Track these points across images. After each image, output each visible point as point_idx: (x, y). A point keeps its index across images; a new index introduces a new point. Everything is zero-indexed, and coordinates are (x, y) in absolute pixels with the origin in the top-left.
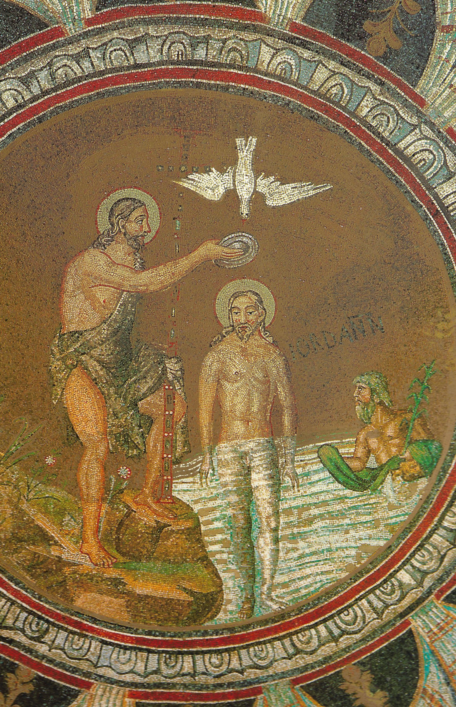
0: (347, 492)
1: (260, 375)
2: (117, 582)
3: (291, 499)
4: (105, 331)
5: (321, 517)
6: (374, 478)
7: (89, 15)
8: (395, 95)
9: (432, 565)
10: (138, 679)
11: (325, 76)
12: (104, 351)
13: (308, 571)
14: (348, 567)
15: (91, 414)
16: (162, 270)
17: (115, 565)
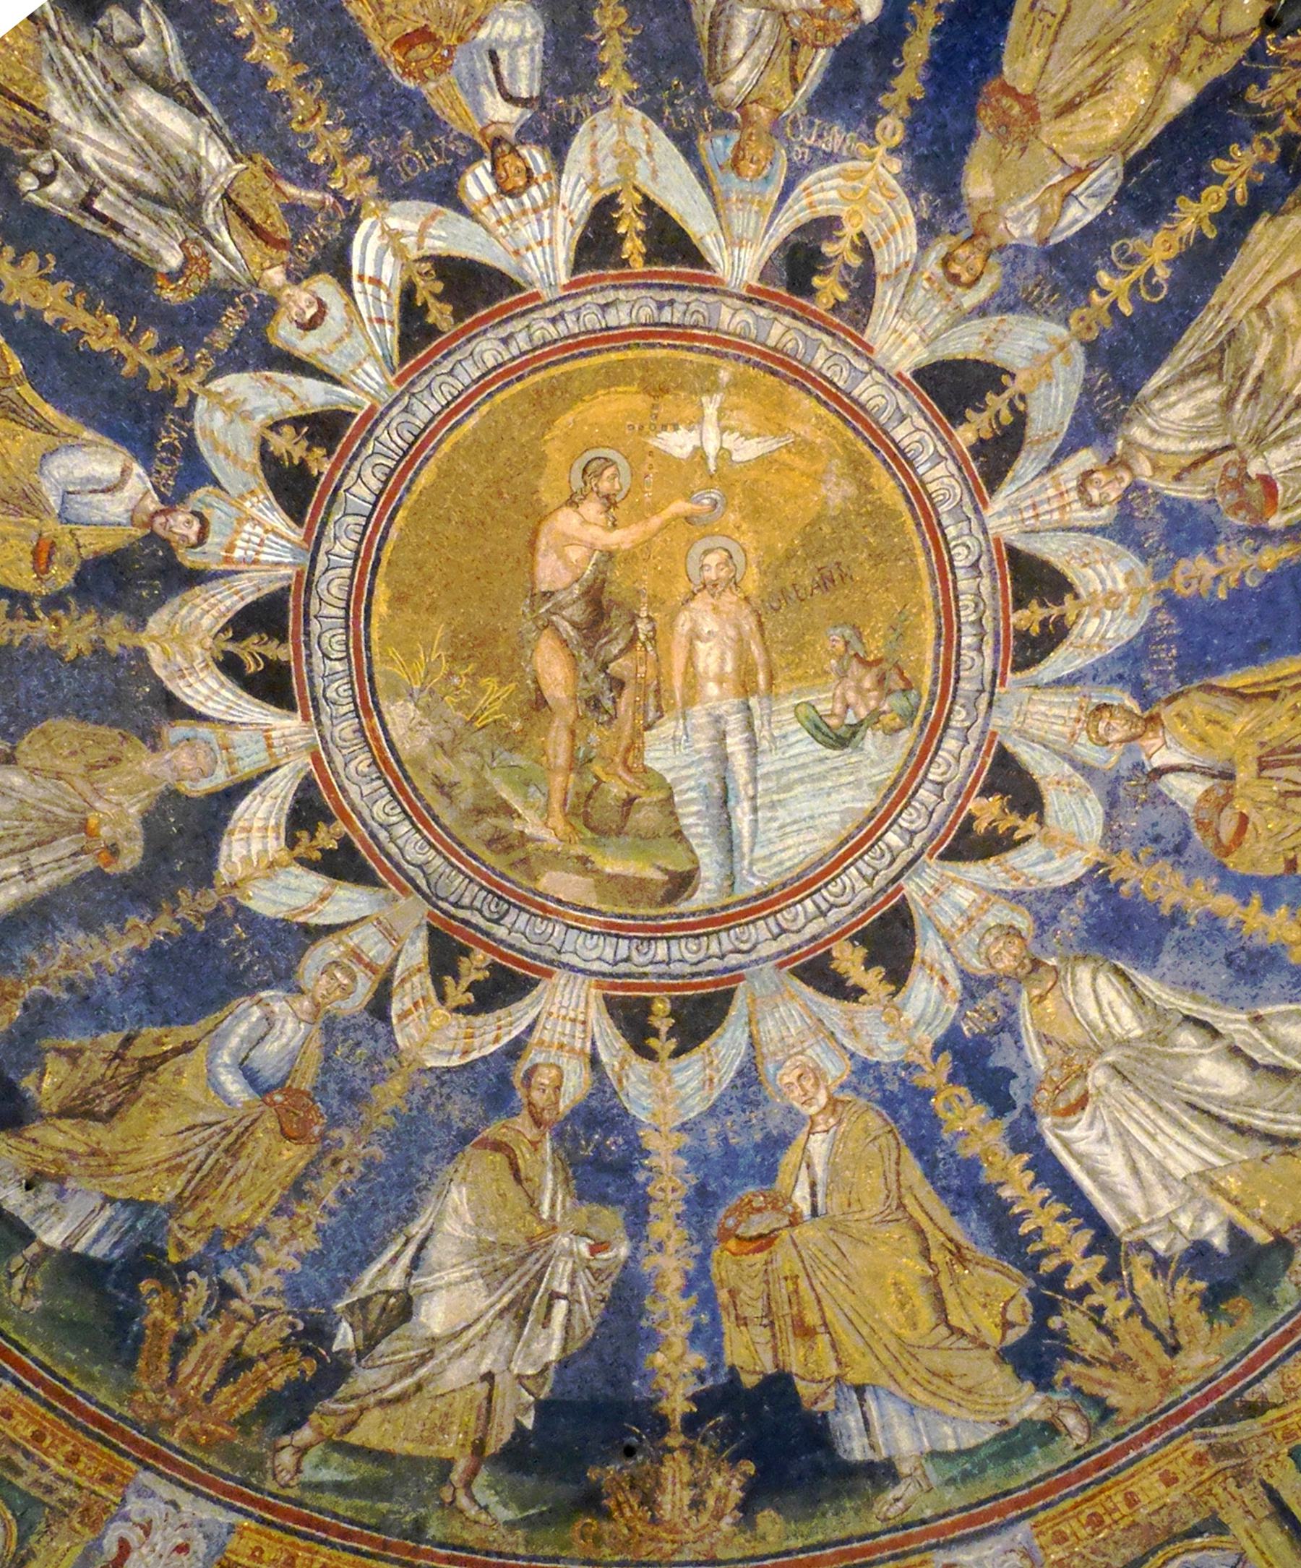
0: (829, 752)
1: (732, 633)
2: (584, 860)
3: (769, 763)
4: (577, 590)
5: (801, 781)
6: (854, 734)
7: (564, 280)
8: (846, 344)
9: (921, 823)
10: (606, 968)
11: (780, 331)
12: (577, 612)
13: (790, 842)
14: (833, 833)
15: (560, 677)
16: (634, 528)
17: (583, 841)
